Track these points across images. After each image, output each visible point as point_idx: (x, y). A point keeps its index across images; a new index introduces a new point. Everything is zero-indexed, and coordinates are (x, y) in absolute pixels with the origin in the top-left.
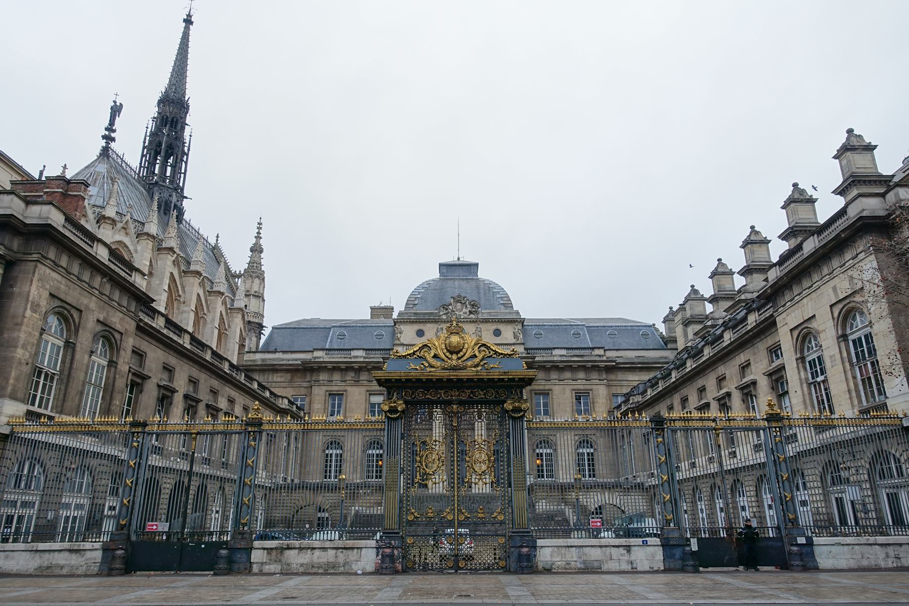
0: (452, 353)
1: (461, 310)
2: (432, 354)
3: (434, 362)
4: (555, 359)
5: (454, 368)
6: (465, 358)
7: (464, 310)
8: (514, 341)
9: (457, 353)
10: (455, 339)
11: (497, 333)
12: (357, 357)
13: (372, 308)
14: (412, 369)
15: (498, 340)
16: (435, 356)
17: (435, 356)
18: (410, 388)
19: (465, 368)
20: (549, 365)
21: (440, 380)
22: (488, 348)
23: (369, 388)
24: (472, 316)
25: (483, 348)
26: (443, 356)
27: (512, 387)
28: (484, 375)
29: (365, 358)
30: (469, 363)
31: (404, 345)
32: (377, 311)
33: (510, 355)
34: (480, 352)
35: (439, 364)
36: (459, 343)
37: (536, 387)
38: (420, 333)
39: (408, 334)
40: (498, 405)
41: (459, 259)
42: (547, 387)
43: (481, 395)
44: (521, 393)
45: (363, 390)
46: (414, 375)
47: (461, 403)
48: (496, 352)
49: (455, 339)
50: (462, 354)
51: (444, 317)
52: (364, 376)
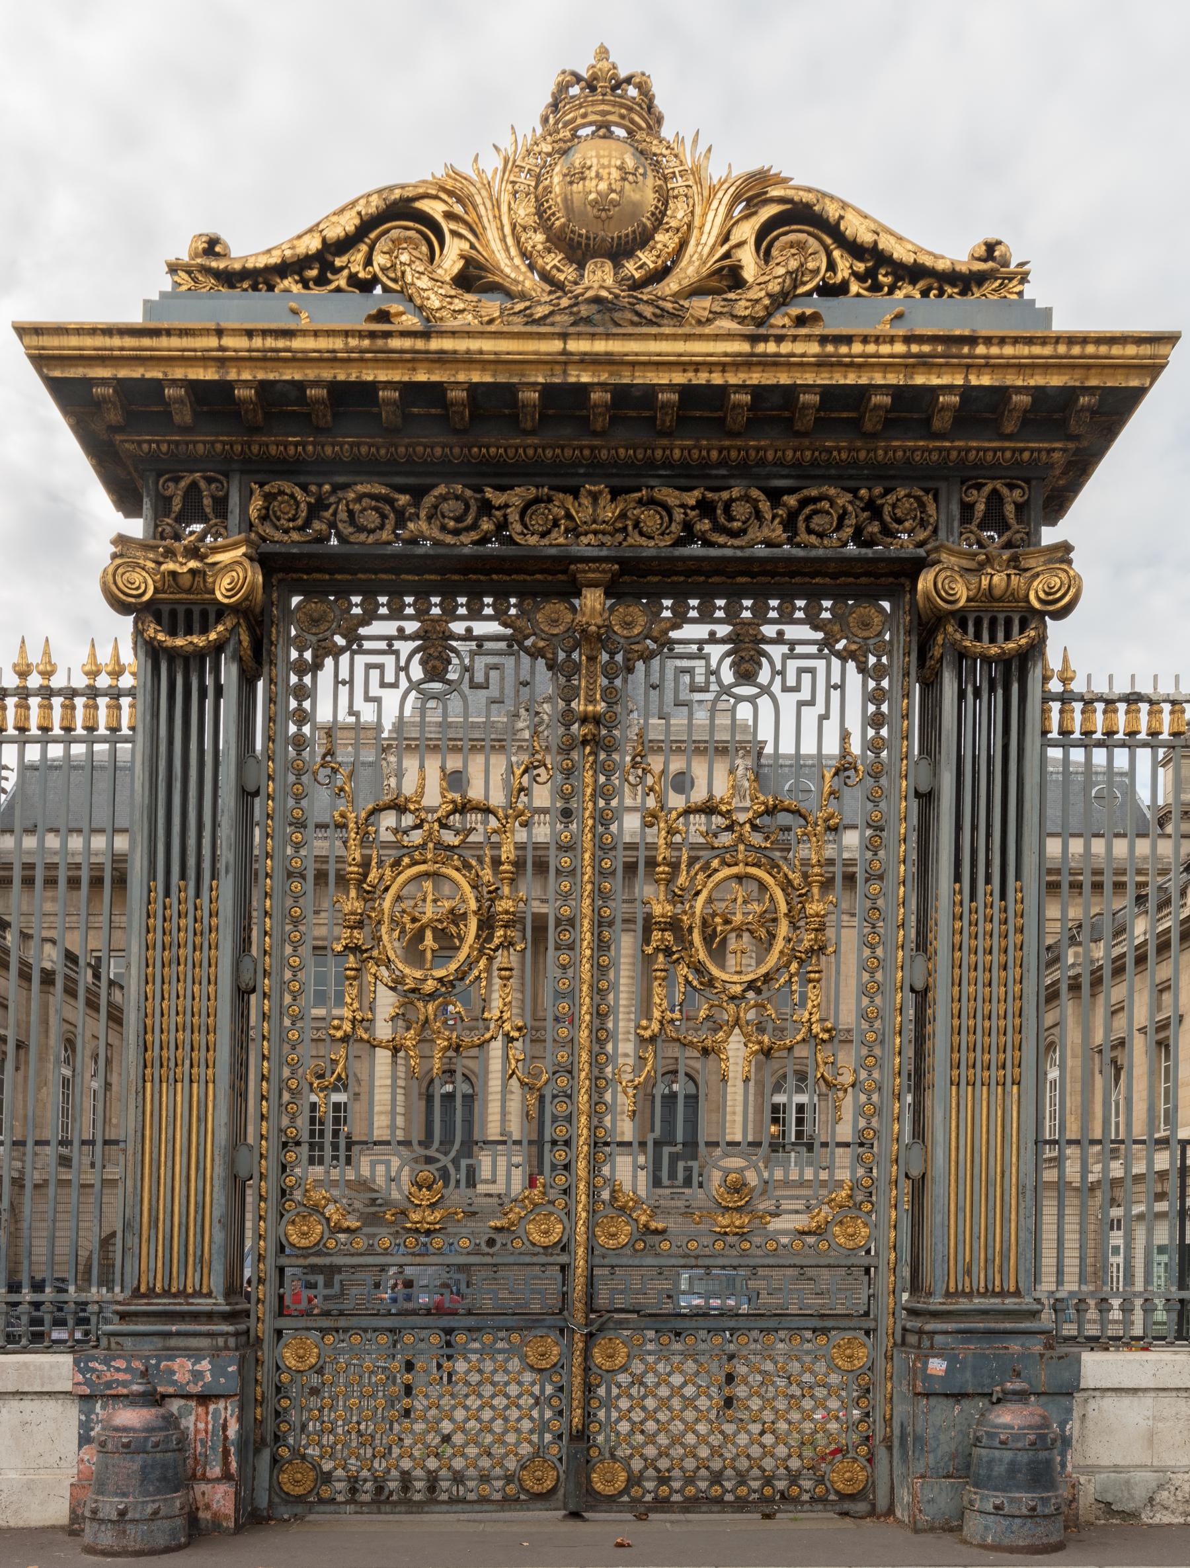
9: (619, 253)
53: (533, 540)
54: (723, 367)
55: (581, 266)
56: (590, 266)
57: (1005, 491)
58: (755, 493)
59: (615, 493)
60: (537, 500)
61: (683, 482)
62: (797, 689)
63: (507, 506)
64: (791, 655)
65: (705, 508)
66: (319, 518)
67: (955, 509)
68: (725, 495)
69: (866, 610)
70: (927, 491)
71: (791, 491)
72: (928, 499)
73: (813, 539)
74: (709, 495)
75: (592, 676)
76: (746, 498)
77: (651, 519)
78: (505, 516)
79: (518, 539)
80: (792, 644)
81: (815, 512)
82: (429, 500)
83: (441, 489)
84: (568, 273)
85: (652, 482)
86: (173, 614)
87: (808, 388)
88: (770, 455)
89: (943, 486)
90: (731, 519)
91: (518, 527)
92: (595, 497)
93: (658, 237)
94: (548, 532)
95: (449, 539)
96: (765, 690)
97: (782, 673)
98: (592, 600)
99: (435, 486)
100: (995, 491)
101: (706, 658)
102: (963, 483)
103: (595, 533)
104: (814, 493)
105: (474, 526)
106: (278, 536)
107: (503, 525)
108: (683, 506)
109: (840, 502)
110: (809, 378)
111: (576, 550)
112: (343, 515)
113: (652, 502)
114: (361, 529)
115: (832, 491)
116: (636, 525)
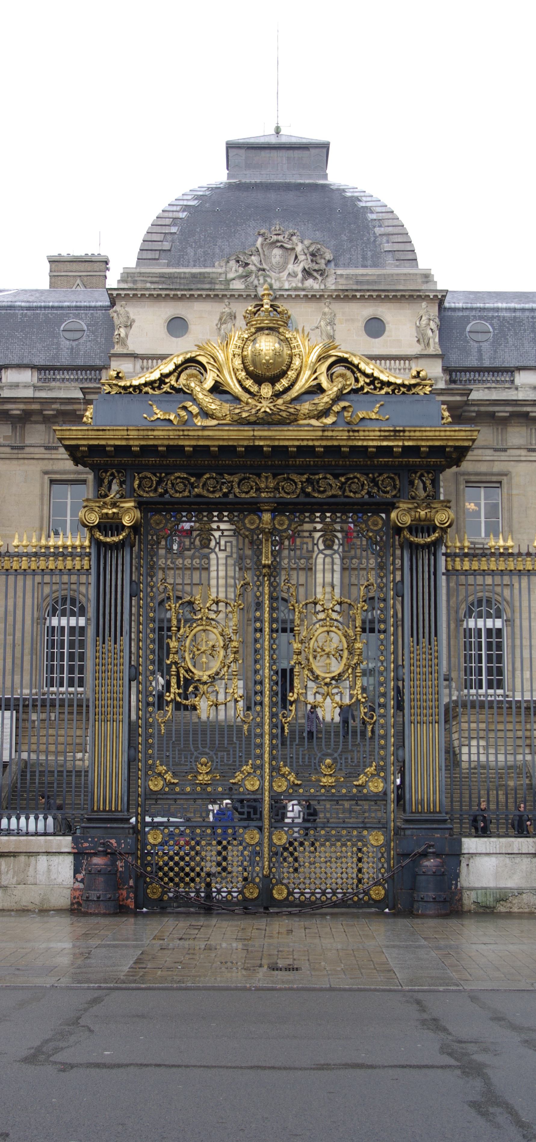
0: (259, 380)
1: (283, 267)
2: (209, 384)
3: (212, 404)
4: (521, 396)
5: (268, 421)
6: (294, 393)
7: (291, 267)
8: (416, 349)
9: (273, 380)
10: (267, 346)
11: (375, 327)
12: (16, 386)
13: (53, 261)
15: (378, 346)
16: (217, 389)
17: (217, 389)
18: (153, 469)
19: (292, 420)
20: (503, 411)
21: (228, 450)
22: (353, 368)
23: (49, 466)
24: (310, 283)
25: (339, 369)
26: (237, 389)
27: (412, 469)
28: (341, 437)
29: (35, 388)
30: (305, 407)
31: (134, 356)
32: (65, 269)
33: (410, 387)
34: (331, 378)
35: (226, 407)
36: (277, 354)
38: (177, 326)
39: (145, 328)
40: (376, 513)
41: (278, 131)
42: (497, 468)
43: (331, 487)
44: (435, 483)
45: (34, 469)
46: (162, 436)
47: (280, 508)
48: (373, 379)
49: (267, 346)
50: (285, 382)
51: (238, 285)
52: (36, 435)
53: (243, 495)
54: (313, 440)
55: (260, 385)
56: (263, 386)
58: (328, 476)
60: (244, 478)
63: (233, 482)
68: (317, 477)
69: (375, 518)
70: (395, 474)
71: (342, 475)
72: (396, 478)
73: (352, 494)
75: (267, 547)
77: (289, 487)
78: (232, 485)
79: (238, 495)
83: (207, 476)
84: (254, 389)
85: (289, 471)
86: (105, 527)
87: (344, 446)
88: (333, 463)
91: (237, 490)
92: (267, 478)
93: (289, 373)
94: (249, 492)
95: (211, 496)
96: (336, 552)
98: (267, 517)
99: (205, 474)
101: (313, 538)
102: (409, 470)
104: (352, 476)
105: (221, 489)
106: (145, 495)
109: (362, 479)
114: (177, 491)
115: (358, 476)
116: (283, 488)
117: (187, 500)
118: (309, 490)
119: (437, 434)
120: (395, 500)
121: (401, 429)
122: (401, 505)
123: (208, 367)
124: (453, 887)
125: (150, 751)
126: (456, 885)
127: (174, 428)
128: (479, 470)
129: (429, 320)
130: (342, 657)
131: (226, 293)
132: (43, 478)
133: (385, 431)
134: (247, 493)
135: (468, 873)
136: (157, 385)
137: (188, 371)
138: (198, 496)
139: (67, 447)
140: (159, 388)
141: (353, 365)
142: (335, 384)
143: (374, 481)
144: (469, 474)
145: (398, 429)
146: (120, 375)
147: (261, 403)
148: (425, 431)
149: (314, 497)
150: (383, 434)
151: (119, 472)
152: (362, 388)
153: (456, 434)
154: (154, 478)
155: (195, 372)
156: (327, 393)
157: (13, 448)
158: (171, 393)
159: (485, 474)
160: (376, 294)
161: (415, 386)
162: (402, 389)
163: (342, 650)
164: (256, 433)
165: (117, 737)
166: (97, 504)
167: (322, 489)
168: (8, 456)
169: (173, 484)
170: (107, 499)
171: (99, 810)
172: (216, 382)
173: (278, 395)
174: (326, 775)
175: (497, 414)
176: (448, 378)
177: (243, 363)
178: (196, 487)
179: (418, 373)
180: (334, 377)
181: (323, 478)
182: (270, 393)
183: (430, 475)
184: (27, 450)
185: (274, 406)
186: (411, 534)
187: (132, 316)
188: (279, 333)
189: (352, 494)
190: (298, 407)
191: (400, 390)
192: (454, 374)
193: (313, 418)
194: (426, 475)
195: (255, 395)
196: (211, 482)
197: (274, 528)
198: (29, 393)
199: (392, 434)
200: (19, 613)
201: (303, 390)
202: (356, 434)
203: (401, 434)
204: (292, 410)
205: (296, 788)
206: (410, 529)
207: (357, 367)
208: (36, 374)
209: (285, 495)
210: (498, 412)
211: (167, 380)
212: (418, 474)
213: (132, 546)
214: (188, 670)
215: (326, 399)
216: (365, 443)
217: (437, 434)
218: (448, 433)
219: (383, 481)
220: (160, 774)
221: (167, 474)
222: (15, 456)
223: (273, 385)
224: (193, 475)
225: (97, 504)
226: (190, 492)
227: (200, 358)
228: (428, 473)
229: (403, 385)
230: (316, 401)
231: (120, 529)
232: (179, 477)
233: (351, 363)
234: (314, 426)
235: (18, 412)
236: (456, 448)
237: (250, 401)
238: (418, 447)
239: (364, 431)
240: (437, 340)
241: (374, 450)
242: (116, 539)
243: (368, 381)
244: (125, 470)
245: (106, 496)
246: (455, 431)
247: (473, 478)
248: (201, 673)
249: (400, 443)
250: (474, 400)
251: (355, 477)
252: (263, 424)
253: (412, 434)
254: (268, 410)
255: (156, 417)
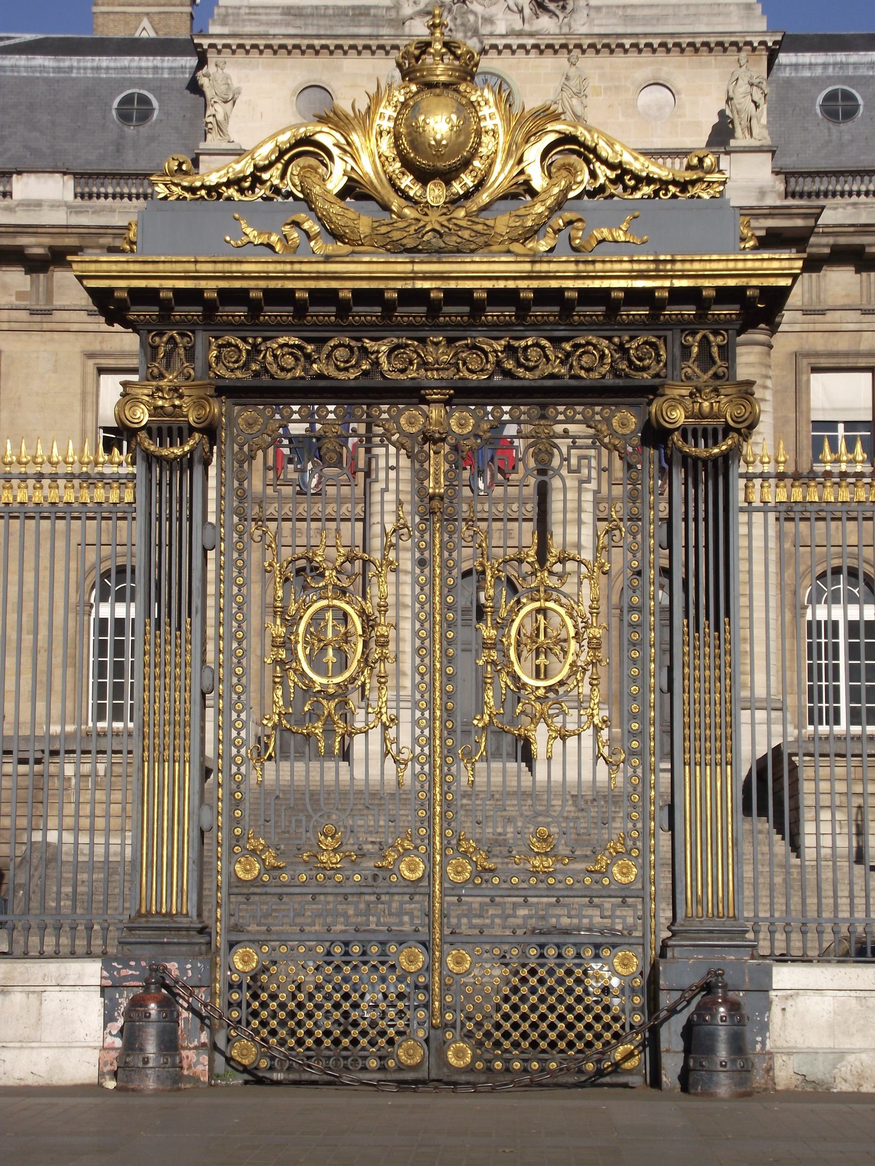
0: (423, 177)
2: (336, 183)
6: (484, 198)
9: (448, 176)
12: (38, 204)
14: (257, 252)
17: (353, 190)
23: (95, 344)
28: (565, 275)
30: (503, 223)
33: (683, 186)
37: (819, 343)
45: (71, 347)
46: (256, 271)
48: (622, 173)
50: (468, 180)
54: (515, 278)
56: (430, 186)
57: (711, 338)
58: (544, 342)
59: (450, 341)
61: (496, 334)
62: (578, 471)
63: (378, 352)
64: (574, 446)
65: (510, 350)
66: (255, 361)
67: (677, 351)
68: (523, 343)
70: (659, 337)
71: (567, 339)
73: (583, 373)
74: (512, 342)
76: (536, 345)
80: (574, 438)
81: (584, 353)
82: (327, 349)
84: (415, 190)
85: (474, 334)
89: (669, 334)
90: (527, 360)
93: (476, 163)
95: (342, 376)
97: (568, 460)
100: (705, 337)
101: (517, 448)
102: (683, 331)
103: (437, 370)
105: (357, 365)
107: (376, 364)
108: (496, 351)
110: (570, 284)
111: (425, 383)
112: (270, 359)
113: (474, 347)
114: (283, 369)
116: (464, 364)
117: (301, 383)
118: (509, 365)
119: (731, 265)
120: (657, 381)
121: (669, 258)
122: (667, 391)
123: (336, 152)
124: (758, 1047)
125: (238, 813)
126: (763, 1043)
127: (276, 258)
128: (835, 349)
129: (752, 85)
130: (566, 653)
131: (397, 42)
132: (84, 365)
133: (639, 262)
134: (402, 371)
135: (784, 1025)
136: (247, 184)
137: (302, 161)
138: (321, 376)
139: (91, 291)
140: (252, 188)
141: (587, 148)
142: (554, 181)
143: (622, 349)
144: (817, 355)
145: (662, 258)
146: (184, 167)
147: (426, 214)
148: (710, 261)
149: (519, 378)
150: (636, 266)
151: (182, 335)
152: (602, 189)
153: (765, 265)
154: (241, 345)
155: (313, 161)
156: (541, 198)
157: (33, 312)
158: (271, 199)
159: (847, 355)
160: (659, 41)
161: (693, 183)
162: (671, 187)
163: (565, 641)
164: (418, 267)
165: (182, 788)
166: (146, 391)
167: (532, 364)
168: (24, 326)
169: (275, 356)
170: (163, 383)
171: (149, 912)
172: (350, 179)
173: (455, 201)
174: (538, 854)
175: (868, 250)
176: (782, 187)
177: (397, 146)
178: (314, 362)
179: (701, 161)
180: (553, 170)
181: (533, 345)
182: (442, 200)
183: (720, 338)
184: (57, 316)
185: (449, 220)
186: (685, 440)
187: (235, 84)
188: (457, 91)
189: (583, 373)
190: (490, 223)
191: (667, 190)
192: (793, 180)
193: (517, 240)
194: (711, 338)
195: (417, 203)
196: (340, 353)
197: (450, 432)
198: (60, 218)
199: (652, 266)
200: (44, 594)
201: (501, 192)
202: (590, 267)
203: (669, 267)
204: (479, 228)
205: (486, 876)
206: (684, 431)
207: (594, 150)
208: (70, 182)
209: (467, 374)
210: (870, 245)
211: (265, 176)
212: (698, 337)
213: (206, 463)
214: (303, 674)
215: (539, 209)
216: (606, 284)
217: (731, 265)
218: (749, 265)
219: (637, 349)
220: (253, 852)
221: (265, 339)
222: (36, 327)
223: (448, 184)
224: (309, 340)
225: (146, 391)
226: (305, 370)
227: (319, 138)
228: (716, 333)
229: (674, 182)
230: (522, 212)
231: (186, 432)
232: (286, 345)
233: (582, 144)
234: (517, 255)
235: (40, 251)
236: (762, 289)
237: (407, 211)
238: (698, 290)
239: (604, 262)
240: (764, 120)
241: (621, 295)
242: (178, 451)
243: (612, 175)
244: (193, 332)
245: (162, 376)
246: (763, 260)
247: (824, 362)
248: (324, 681)
249: (667, 283)
250: (827, 226)
251: (588, 343)
252: (429, 252)
253: (687, 266)
254: (438, 228)
255: (245, 239)
